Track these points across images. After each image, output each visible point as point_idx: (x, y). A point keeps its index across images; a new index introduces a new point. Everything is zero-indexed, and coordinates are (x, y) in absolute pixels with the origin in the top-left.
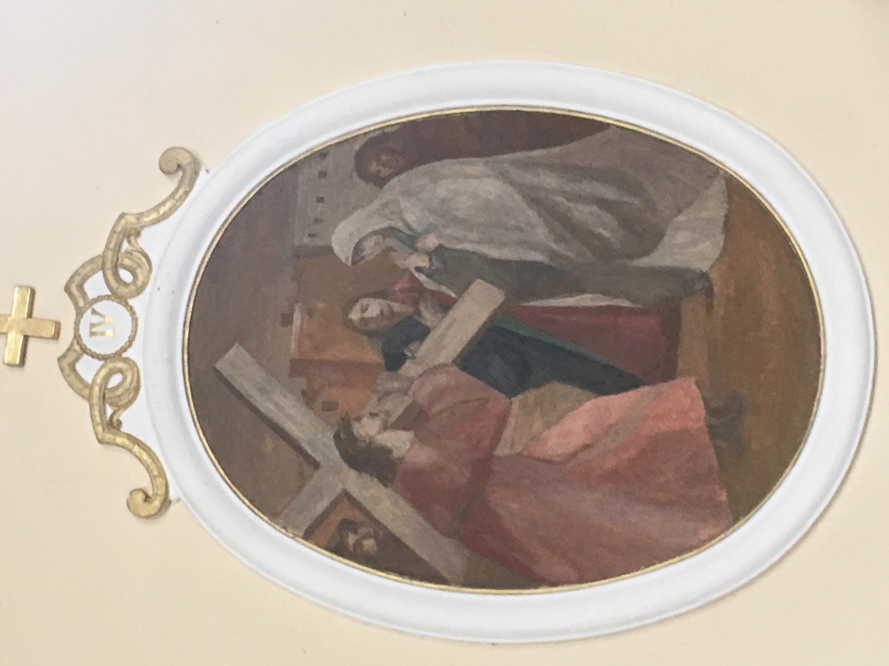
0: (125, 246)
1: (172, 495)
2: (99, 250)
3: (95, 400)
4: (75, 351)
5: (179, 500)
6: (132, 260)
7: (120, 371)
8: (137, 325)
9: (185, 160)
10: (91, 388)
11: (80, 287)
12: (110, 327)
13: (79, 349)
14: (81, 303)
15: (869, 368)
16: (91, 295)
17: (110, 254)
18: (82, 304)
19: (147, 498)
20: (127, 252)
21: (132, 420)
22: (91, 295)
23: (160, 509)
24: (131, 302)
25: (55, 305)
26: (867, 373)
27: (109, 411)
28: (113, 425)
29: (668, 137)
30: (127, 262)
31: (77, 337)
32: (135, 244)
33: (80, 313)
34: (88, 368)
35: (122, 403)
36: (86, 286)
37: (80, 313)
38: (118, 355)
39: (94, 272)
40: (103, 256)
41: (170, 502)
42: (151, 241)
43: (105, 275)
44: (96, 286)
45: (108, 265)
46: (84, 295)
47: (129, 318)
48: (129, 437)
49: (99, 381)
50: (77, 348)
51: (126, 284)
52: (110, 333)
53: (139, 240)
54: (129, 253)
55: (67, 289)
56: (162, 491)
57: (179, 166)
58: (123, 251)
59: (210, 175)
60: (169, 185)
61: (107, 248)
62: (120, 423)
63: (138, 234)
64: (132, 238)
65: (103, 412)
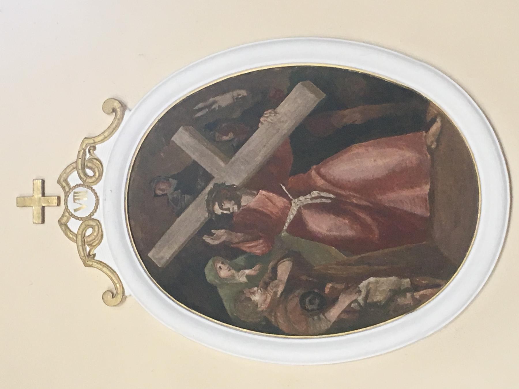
0: (88, 156)
1: (127, 294)
2: (74, 159)
3: (80, 244)
4: (66, 216)
5: (130, 295)
6: (93, 164)
7: (92, 227)
8: (97, 207)
9: (117, 105)
10: (77, 237)
11: (66, 181)
12: (84, 204)
13: (68, 214)
14: (67, 190)
15: (501, 241)
16: (72, 184)
17: (80, 161)
18: (67, 188)
19: (113, 297)
20: (89, 159)
21: (101, 253)
22: (72, 184)
23: (119, 304)
24: (94, 187)
25: (53, 189)
26: (495, 255)
27: (88, 249)
28: (91, 256)
29: (332, 337)
30: (89, 165)
31: (67, 208)
32: (93, 155)
33: (67, 196)
34: (74, 225)
35: (94, 244)
36: (69, 180)
37: (67, 196)
38: (90, 217)
39: (71, 172)
40: (76, 162)
41: (126, 297)
42: (102, 151)
43: (79, 174)
44: (74, 179)
45: (80, 167)
46: (68, 184)
47: (92, 208)
48: (100, 262)
49: (80, 233)
50: (67, 214)
51: (91, 177)
52: (84, 206)
53: (95, 152)
54: (90, 160)
55: (59, 182)
56: (120, 291)
57: (114, 110)
58: (87, 159)
59: (132, 111)
60: (111, 118)
61: (78, 158)
62: (94, 255)
63: (95, 148)
64: (91, 151)
65: (84, 249)
